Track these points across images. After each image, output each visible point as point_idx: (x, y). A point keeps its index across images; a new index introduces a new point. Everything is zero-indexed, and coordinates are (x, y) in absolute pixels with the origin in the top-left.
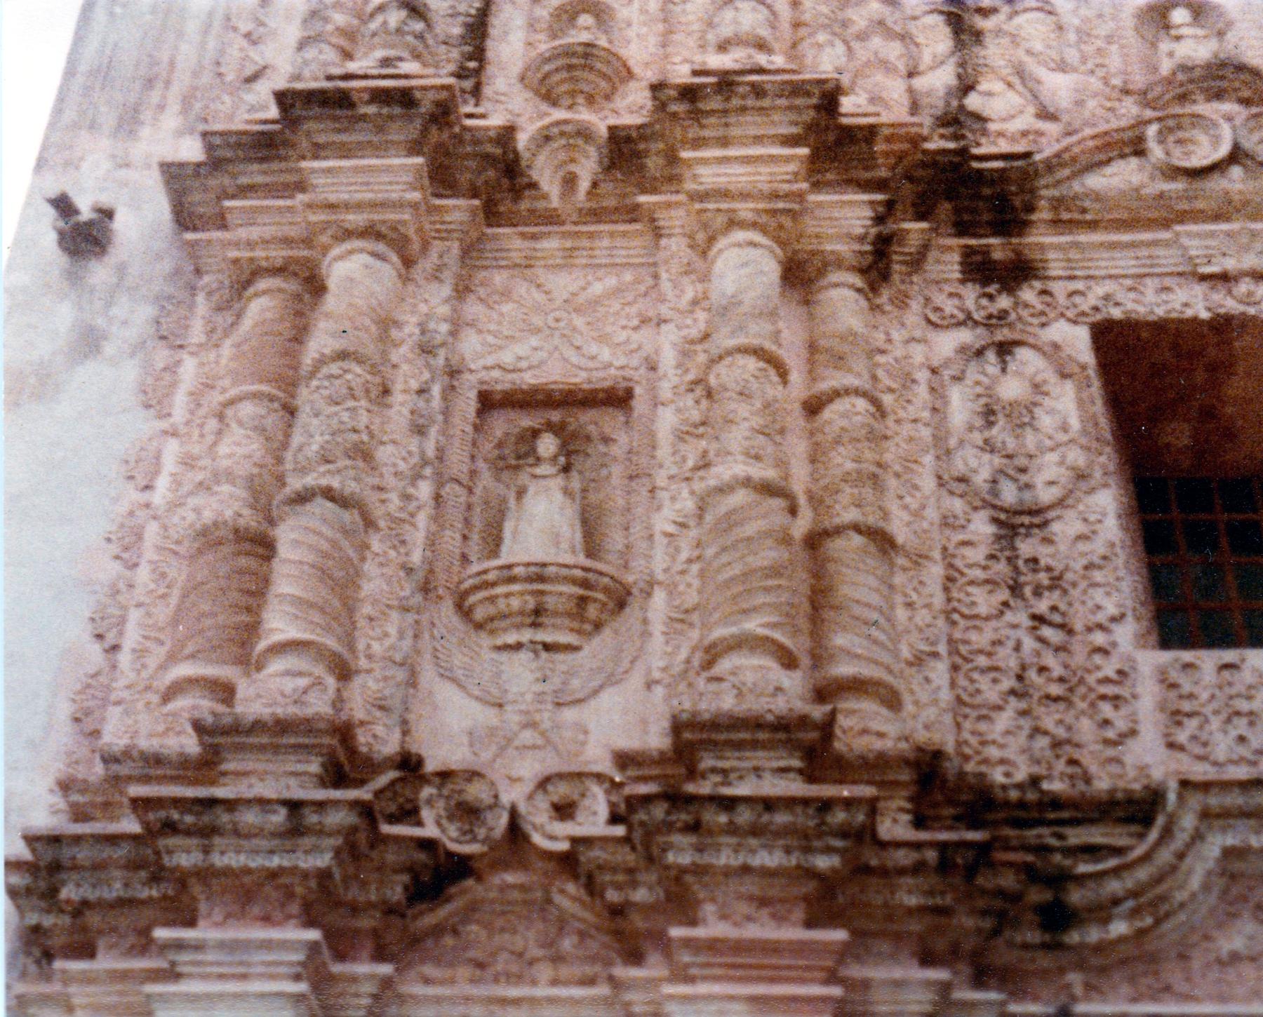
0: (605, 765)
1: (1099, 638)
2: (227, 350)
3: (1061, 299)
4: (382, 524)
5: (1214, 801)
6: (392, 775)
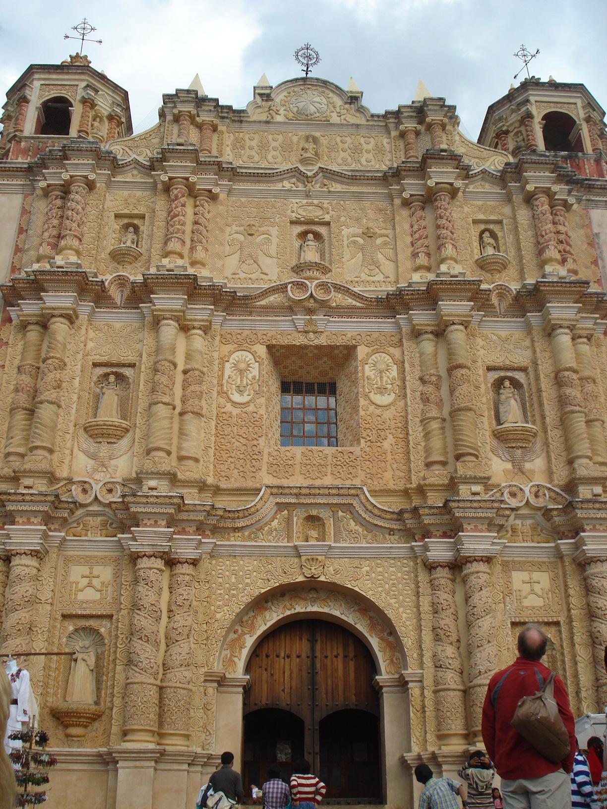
0: (120, 480)
1: (255, 442)
2: (20, 346)
3: (260, 338)
4: (64, 407)
5: (275, 491)
6: (65, 482)
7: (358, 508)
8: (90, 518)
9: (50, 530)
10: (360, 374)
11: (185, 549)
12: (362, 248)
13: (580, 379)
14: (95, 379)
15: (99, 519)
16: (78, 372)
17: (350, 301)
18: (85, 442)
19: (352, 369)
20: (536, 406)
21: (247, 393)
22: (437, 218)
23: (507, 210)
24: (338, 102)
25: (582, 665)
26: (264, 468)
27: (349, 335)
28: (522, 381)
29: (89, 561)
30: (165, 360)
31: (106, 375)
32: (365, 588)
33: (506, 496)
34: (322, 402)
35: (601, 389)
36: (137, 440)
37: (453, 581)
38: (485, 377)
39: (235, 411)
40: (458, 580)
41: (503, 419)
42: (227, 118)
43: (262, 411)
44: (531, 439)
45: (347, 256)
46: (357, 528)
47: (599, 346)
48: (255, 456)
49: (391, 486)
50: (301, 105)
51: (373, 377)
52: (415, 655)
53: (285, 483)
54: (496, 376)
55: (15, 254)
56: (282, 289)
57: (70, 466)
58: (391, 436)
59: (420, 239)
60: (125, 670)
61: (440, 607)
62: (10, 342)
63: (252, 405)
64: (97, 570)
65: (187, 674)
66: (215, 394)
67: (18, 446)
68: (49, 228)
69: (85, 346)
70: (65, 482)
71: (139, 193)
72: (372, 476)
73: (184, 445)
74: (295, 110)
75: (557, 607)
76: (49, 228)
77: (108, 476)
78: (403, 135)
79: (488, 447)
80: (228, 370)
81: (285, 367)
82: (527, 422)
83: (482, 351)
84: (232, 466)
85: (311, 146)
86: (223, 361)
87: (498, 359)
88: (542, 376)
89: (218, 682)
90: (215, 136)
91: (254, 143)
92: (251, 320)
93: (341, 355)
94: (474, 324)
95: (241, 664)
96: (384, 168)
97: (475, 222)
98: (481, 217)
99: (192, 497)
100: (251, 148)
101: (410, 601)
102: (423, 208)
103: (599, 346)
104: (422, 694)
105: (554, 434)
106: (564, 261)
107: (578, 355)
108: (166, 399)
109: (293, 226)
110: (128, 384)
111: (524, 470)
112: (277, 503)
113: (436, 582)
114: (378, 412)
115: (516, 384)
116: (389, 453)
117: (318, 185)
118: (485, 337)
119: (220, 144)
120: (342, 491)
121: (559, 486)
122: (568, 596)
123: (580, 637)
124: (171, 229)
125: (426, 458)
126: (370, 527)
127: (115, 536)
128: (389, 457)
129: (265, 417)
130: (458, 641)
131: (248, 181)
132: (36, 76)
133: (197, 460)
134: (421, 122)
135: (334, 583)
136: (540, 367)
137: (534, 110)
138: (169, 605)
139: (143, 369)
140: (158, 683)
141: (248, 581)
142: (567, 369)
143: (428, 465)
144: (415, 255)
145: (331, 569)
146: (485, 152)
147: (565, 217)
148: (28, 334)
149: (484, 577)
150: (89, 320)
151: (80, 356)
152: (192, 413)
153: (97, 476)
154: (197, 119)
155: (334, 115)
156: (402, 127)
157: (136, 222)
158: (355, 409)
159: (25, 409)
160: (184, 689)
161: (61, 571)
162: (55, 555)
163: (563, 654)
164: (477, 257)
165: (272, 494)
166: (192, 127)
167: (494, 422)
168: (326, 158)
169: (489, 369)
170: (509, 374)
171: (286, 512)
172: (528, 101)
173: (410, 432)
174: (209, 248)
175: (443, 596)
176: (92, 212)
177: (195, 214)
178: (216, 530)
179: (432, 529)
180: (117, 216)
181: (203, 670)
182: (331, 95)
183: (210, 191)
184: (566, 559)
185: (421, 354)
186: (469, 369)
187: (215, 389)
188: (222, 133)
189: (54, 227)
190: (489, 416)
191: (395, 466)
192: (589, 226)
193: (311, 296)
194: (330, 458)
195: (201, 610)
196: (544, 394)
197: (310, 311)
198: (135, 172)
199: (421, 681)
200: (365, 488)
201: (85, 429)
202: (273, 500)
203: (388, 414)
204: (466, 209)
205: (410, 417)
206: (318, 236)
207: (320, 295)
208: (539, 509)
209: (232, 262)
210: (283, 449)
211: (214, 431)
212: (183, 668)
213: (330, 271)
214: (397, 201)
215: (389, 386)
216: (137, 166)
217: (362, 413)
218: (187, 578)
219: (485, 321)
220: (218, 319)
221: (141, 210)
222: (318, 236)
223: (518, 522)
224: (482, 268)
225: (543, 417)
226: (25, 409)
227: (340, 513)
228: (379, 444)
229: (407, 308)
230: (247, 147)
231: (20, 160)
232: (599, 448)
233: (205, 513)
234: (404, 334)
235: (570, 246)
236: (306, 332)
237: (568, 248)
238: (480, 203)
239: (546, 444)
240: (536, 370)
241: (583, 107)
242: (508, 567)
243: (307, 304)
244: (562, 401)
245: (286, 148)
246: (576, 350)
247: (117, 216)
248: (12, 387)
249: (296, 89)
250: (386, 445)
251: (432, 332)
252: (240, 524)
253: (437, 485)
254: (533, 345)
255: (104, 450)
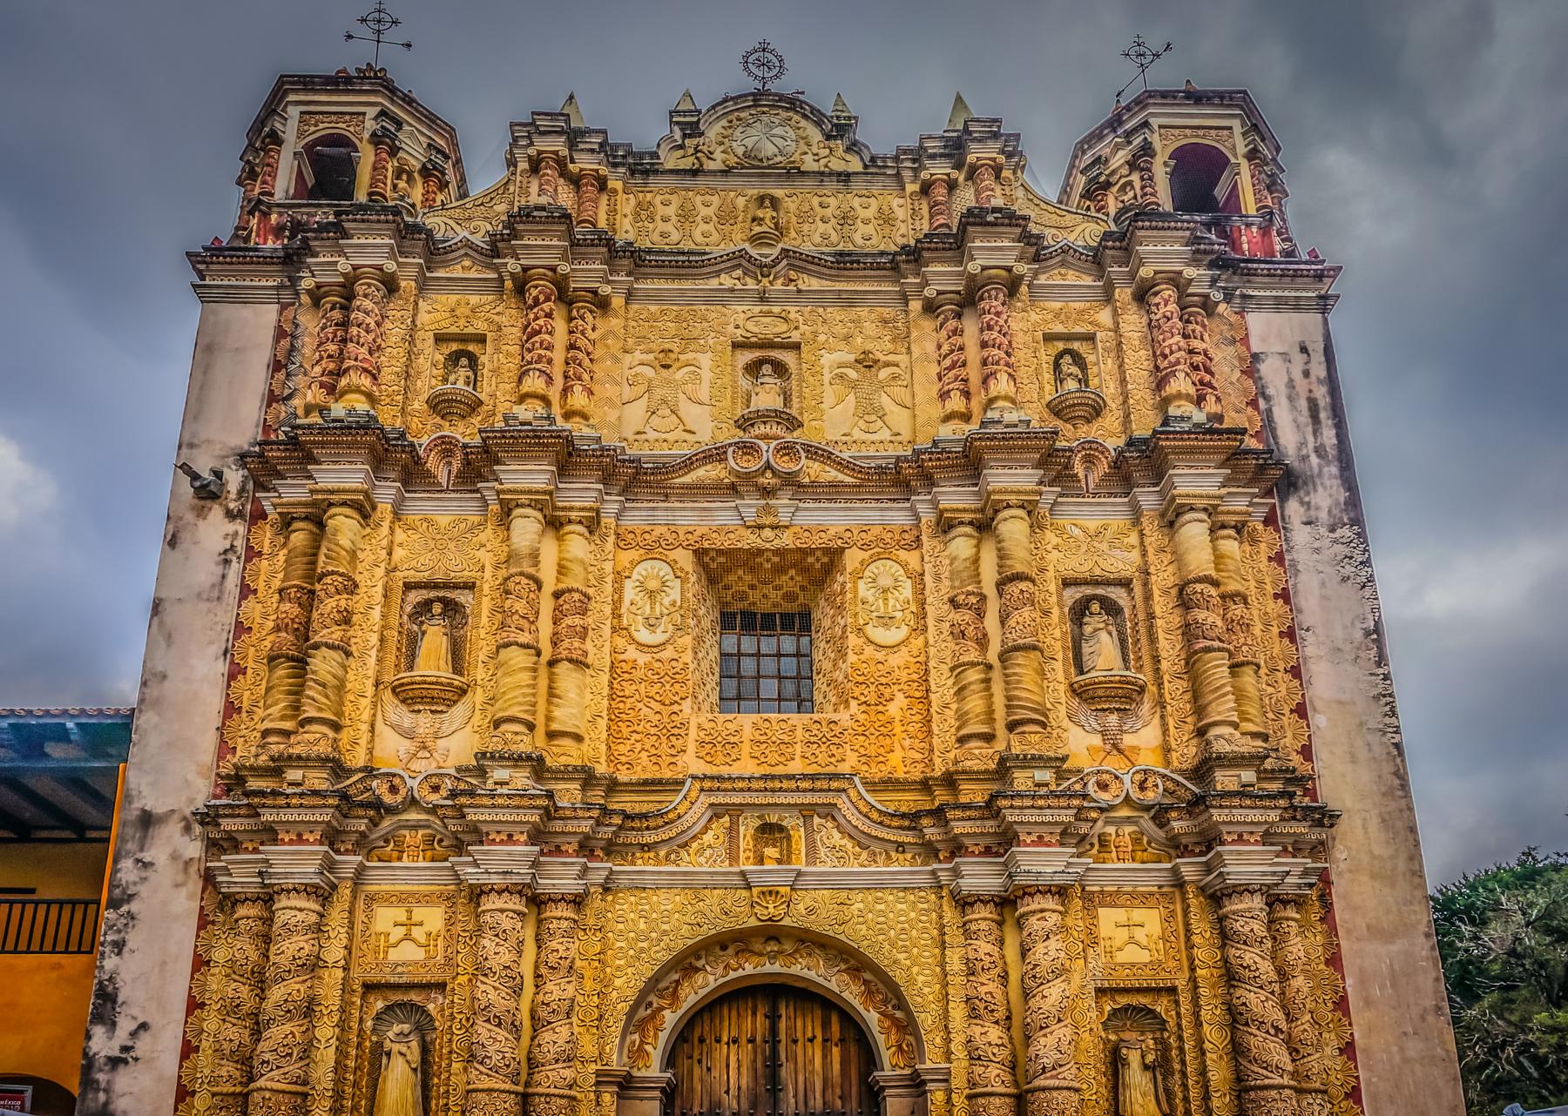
0: (452, 772)
1: (676, 708)
3: (682, 537)
5: (707, 784)
7: (845, 811)
8: (406, 832)
9: (338, 852)
10: (849, 596)
11: (562, 877)
12: (854, 386)
13: (1223, 597)
14: (408, 609)
15: (421, 832)
16: (379, 597)
17: (833, 474)
18: (395, 711)
19: (837, 587)
20: (1144, 641)
21: (662, 628)
22: (982, 330)
23: (1105, 317)
24: (815, 135)
25: (1214, 1057)
26: (692, 747)
27: (832, 532)
28: (1121, 602)
29: (402, 899)
30: (522, 574)
31: (427, 605)
32: (857, 934)
33: (1092, 789)
34: (788, 643)
35: (1255, 613)
36: (478, 706)
37: (1000, 924)
38: (1060, 596)
39: (642, 659)
40: (1010, 922)
41: (1087, 665)
42: (623, 165)
43: (688, 657)
44: (1135, 696)
45: (829, 397)
46: (844, 842)
47: (1254, 542)
48: (674, 731)
49: (900, 775)
50: (750, 142)
51: (871, 599)
52: (938, 1040)
53: (725, 771)
54: (1078, 596)
55: (269, 406)
56: (716, 455)
57: (370, 751)
58: (900, 696)
59: (950, 369)
60: (465, 1069)
61: (979, 965)
62: (265, 551)
63: (670, 648)
64: (419, 913)
65: (568, 1073)
66: (607, 631)
67: (283, 718)
68: (321, 358)
69: (390, 554)
70: (360, 775)
71: (474, 299)
72: (867, 759)
73: (557, 713)
74: (740, 151)
75: (1172, 964)
76: (321, 358)
77: (434, 765)
78: (926, 189)
79: (1063, 709)
80: (630, 591)
81: (727, 588)
82: (1127, 669)
83: (1055, 554)
84: (639, 746)
85: (768, 213)
86: (620, 577)
87: (1079, 565)
88: (1156, 593)
89: (619, 1084)
90: (604, 199)
91: (671, 211)
92: (667, 509)
93: (818, 566)
94: (1043, 508)
95: (656, 1054)
96: (894, 248)
97: (1049, 338)
98: (1059, 328)
99: (568, 794)
100: (665, 220)
101: (929, 955)
102: (959, 316)
103: (1254, 542)
104: (949, 1100)
105: (1175, 689)
106: (1199, 401)
107: (1218, 558)
108: (524, 638)
109: (738, 352)
110: (465, 616)
111: (1122, 746)
112: (711, 805)
113: (973, 927)
114: (880, 656)
115: (1111, 608)
116: (897, 724)
117: (780, 281)
118: (1060, 531)
119: (612, 211)
120: (818, 784)
121: (1181, 772)
122: (1190, 946)
123: (1211, 1012)
124: (528, 357)
125: (959, 729)
126: (863, 841)
127: (446, 860)
128: (898, 729)
129: (692, 667)
130: (1008, 1018)
131: (660, 276)
132: (292, 97)
133: (578, 738)
134: (958, 166)
135: (807, 930)
136: (1154, 578)
137: (1156, 140)
138: (537, 967)
139: (486, 590)
140: (520, 1089)
141: (666, 927)
142: (1199, 580)
143: (962, 740)
144: (944, 396)
145: (801, 907)
146: (1069, 216)
147: (1204, 326)
148: (293, 536)
149: (1054, 918)
150: (395, 513)
151: (380, 572)
152: (570, 661)
153: (415, 765)
154: (571, 166)
155: (809, 158)
156: (924, 175)
157: (471, 348)
158: (842, 653)
159: (292, 659)
160: (562, 1097)
161: (360, 917)
162: (348, 891)
163: (1180, 1038)
164: (1049, 398)
165: (702, 790)
166: (562, 181)
167: (1072, 670)
168: (793, 234)
169: (1067, 583)
170: (1100, 591)
171: (727, 818)
172: (1146, 124)
173: (933, 688)
174: (596, 389)
175: (984, 947)
176: (395, 332)
177: (571, 332)
178: (611, 849)
179: (967, 842)
180: (440, 339)
181: (593, 1067)
182: (803, 123)
183: (594, 292)
184: (1190, 888)
185: (953, 560)
186: (1033, 581)
187: (608, 622)
188: (615, 191)
189: (330, 356)
190: (1065, 659)
191: (907, 743)
192: (1245, 340)
193: (768, 466)
194: (799, 732)
195: (588, 974)
196: (1159, 622)
197: (767, 492)
198: (467, 263)
199: (946, 1081)
200: (856, 779)
201: (393, 690)
202: (705, 800)
203: (895, 660)
204: (1034, 317)
205: (932, 664)
206: (780, 369)
207: (784, 465)
208: (1147, 808)
209: (635, 414)
210: (722, 717)
211: (606, 691)
212: (560, 1065)
213: (801, 425)
214: (916, 306)
215: (899, 615)
216: (470, 252)
217: (852, 658)
218: (564, 924)
219: (1062, 504)
220: (611, 506)
221: (480, 326)
222: (780, 369)
223: (1111, 830)
224: (1057, 414)
225: (1156, 659)
226: (292, 659)
227: (817, 820)
228: (880, 708)
229: (929, 481)
230: (658, 218)
231: (270, 244)
232: (1251, 710)
233: (592, 822)
234: (924, 528)
235: (1212, 374)
236: (761, 527)
237: (1208, 378)
238: (1057, 305)
239: (1161, 704)
240: (1146, 584)
241: (1244, 134)
242: (1092, 901)
243: (761, 480)
244: (1189, 632)
245: (726, 217)
246: (1215, 549)
247: (440, 339)
248: (271, 624)
249: (742, 115)
250: (894, 709)
251: (971, 523)
252: (650, 837)
253: (977, 772)
254: (1142, 543)
255: (424, 722)
